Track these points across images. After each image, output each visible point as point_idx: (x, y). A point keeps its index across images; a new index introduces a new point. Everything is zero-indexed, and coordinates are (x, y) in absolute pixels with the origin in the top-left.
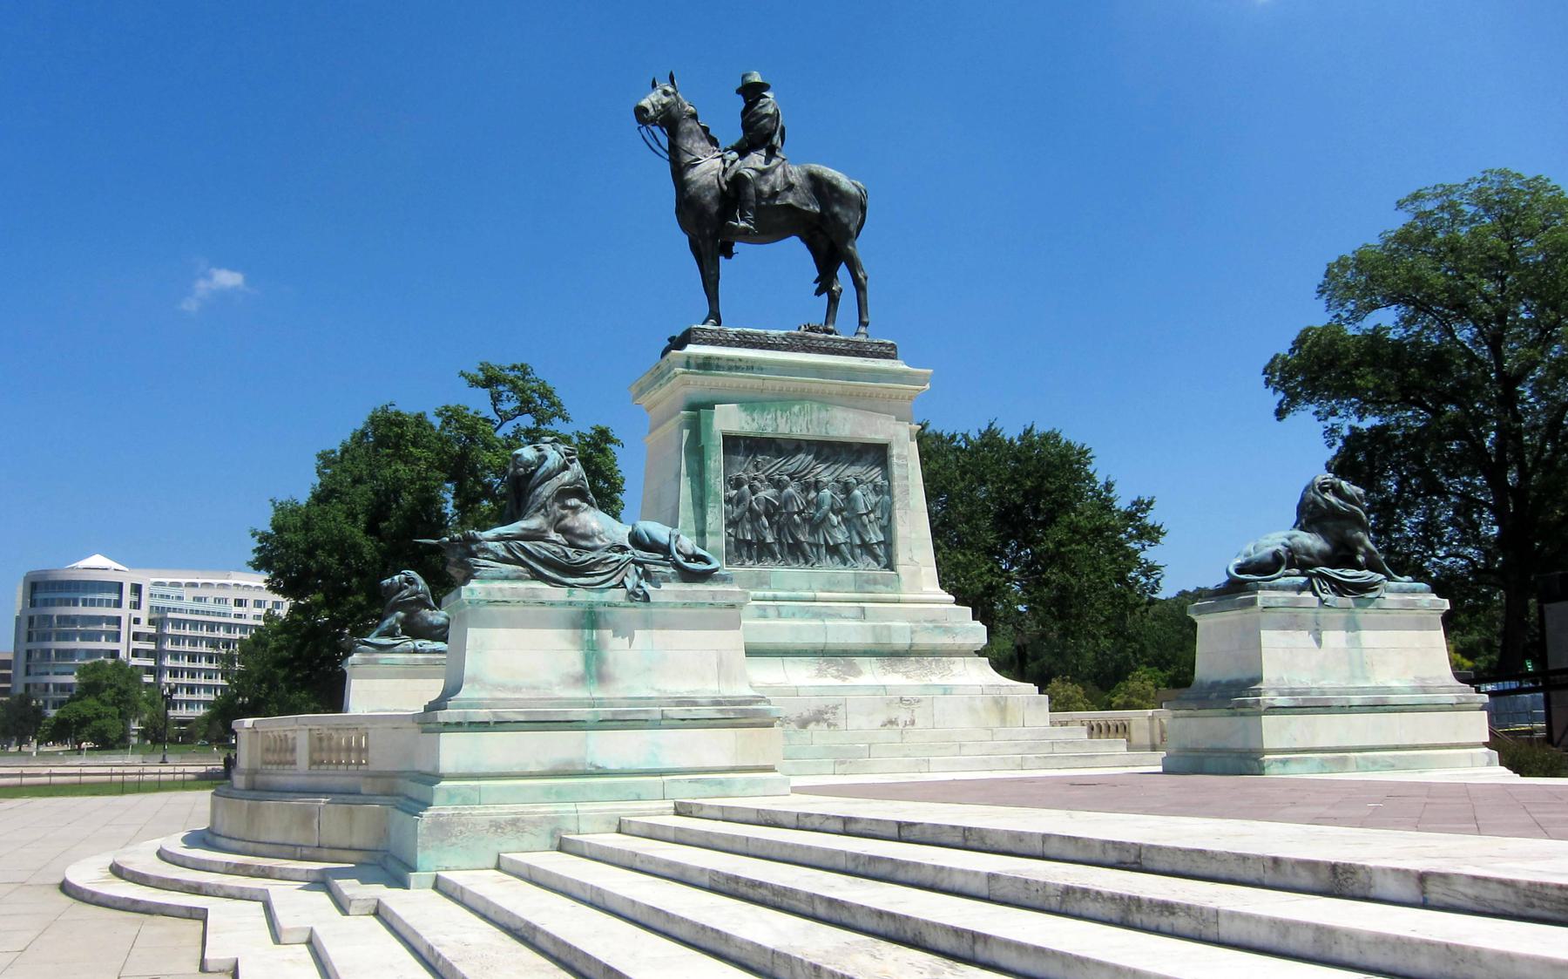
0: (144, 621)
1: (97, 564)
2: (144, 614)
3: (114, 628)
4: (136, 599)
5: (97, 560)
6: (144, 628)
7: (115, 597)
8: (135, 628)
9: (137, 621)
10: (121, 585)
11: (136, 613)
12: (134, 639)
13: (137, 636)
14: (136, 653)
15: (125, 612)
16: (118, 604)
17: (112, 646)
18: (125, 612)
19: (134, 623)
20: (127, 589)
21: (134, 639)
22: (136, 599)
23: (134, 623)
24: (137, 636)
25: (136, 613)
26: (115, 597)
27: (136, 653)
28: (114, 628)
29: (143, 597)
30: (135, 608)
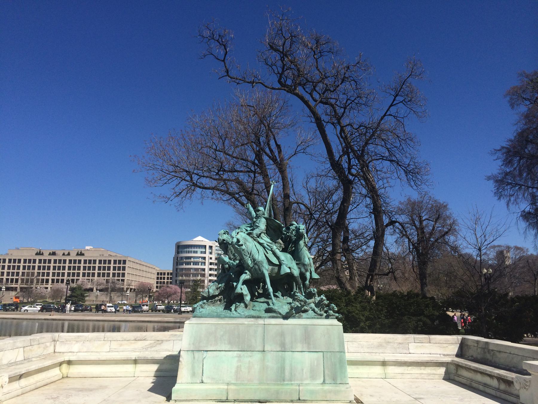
0: (214, 258)
1: (199, 240)
2: (214, 256)
3: (204, 261)
4: (211, 251)
5: (200, 238)
6: (213, 261)
7: (204, 250)
8: (211, 261)
9: (211, 258)
10: (205, 246)
11: (211, 256)
12: (210, 265)
13: (211, 264)
14: (211, 269)
15: (207, 255)
16: (205, 253)
17: (203, 267)
18: (207, 255)
19: (210, 259)
20: (207, 247)
21: (210, 265)
22: (211, 251)
23: (210, 259)
24: (211, 264)
25: (211, 256)
26: (204, 250)
27: (211, 269)
28: (204, 261)
29: (213, 250)
30: (210, 254)
